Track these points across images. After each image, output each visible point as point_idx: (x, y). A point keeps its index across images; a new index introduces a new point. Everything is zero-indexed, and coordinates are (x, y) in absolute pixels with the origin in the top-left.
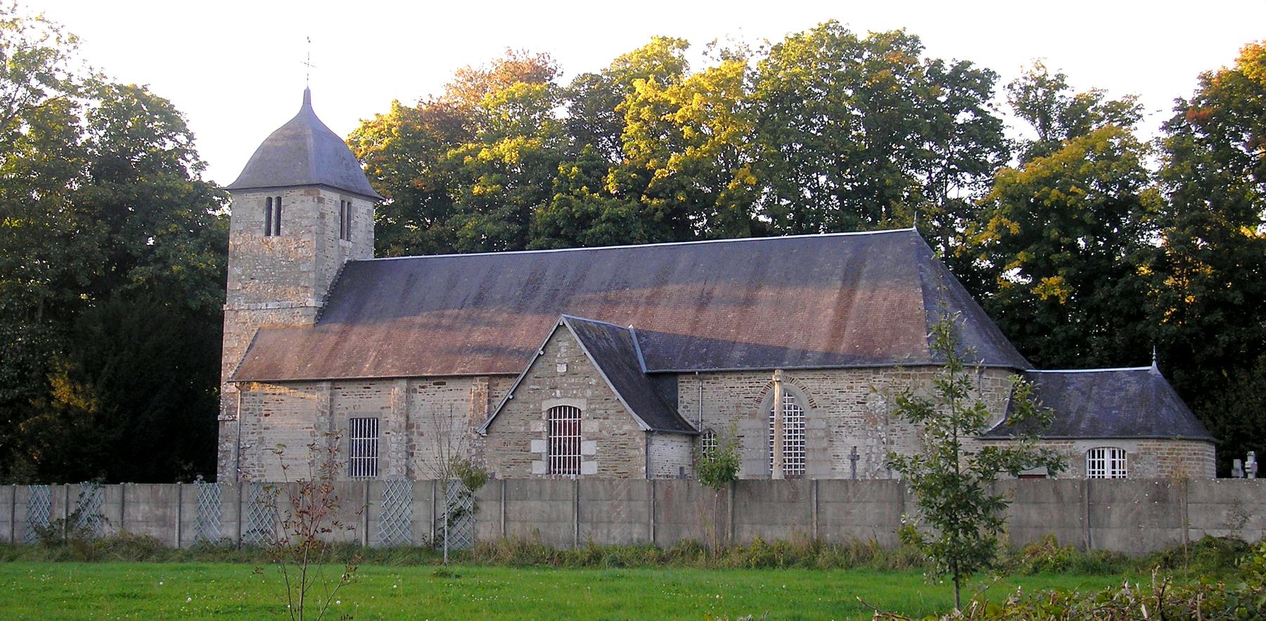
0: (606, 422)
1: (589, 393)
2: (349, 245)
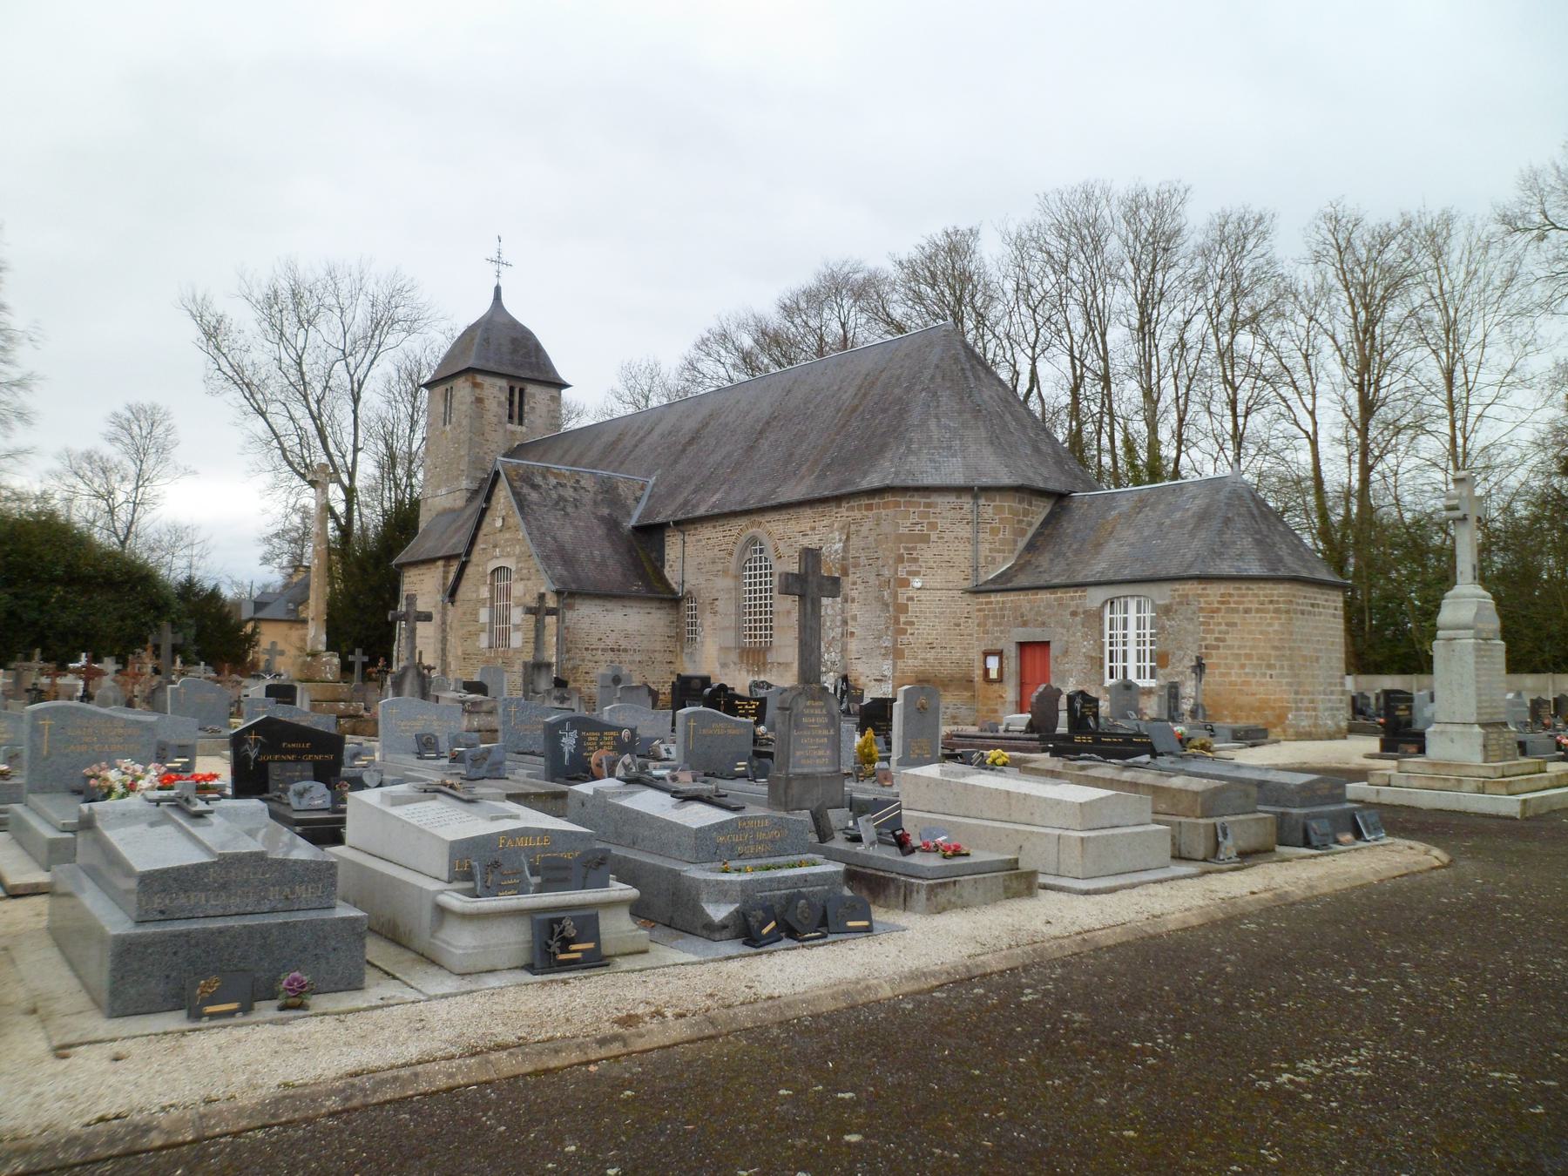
0: (530, 583)
1: (517, 549)
2: (524, 429)
